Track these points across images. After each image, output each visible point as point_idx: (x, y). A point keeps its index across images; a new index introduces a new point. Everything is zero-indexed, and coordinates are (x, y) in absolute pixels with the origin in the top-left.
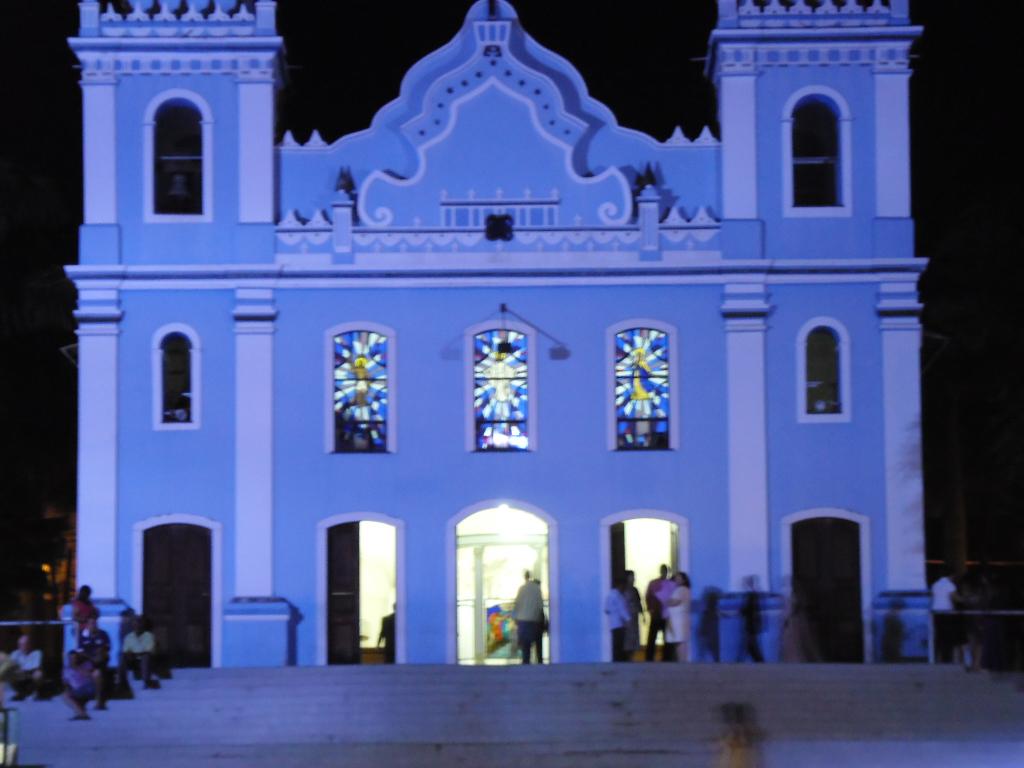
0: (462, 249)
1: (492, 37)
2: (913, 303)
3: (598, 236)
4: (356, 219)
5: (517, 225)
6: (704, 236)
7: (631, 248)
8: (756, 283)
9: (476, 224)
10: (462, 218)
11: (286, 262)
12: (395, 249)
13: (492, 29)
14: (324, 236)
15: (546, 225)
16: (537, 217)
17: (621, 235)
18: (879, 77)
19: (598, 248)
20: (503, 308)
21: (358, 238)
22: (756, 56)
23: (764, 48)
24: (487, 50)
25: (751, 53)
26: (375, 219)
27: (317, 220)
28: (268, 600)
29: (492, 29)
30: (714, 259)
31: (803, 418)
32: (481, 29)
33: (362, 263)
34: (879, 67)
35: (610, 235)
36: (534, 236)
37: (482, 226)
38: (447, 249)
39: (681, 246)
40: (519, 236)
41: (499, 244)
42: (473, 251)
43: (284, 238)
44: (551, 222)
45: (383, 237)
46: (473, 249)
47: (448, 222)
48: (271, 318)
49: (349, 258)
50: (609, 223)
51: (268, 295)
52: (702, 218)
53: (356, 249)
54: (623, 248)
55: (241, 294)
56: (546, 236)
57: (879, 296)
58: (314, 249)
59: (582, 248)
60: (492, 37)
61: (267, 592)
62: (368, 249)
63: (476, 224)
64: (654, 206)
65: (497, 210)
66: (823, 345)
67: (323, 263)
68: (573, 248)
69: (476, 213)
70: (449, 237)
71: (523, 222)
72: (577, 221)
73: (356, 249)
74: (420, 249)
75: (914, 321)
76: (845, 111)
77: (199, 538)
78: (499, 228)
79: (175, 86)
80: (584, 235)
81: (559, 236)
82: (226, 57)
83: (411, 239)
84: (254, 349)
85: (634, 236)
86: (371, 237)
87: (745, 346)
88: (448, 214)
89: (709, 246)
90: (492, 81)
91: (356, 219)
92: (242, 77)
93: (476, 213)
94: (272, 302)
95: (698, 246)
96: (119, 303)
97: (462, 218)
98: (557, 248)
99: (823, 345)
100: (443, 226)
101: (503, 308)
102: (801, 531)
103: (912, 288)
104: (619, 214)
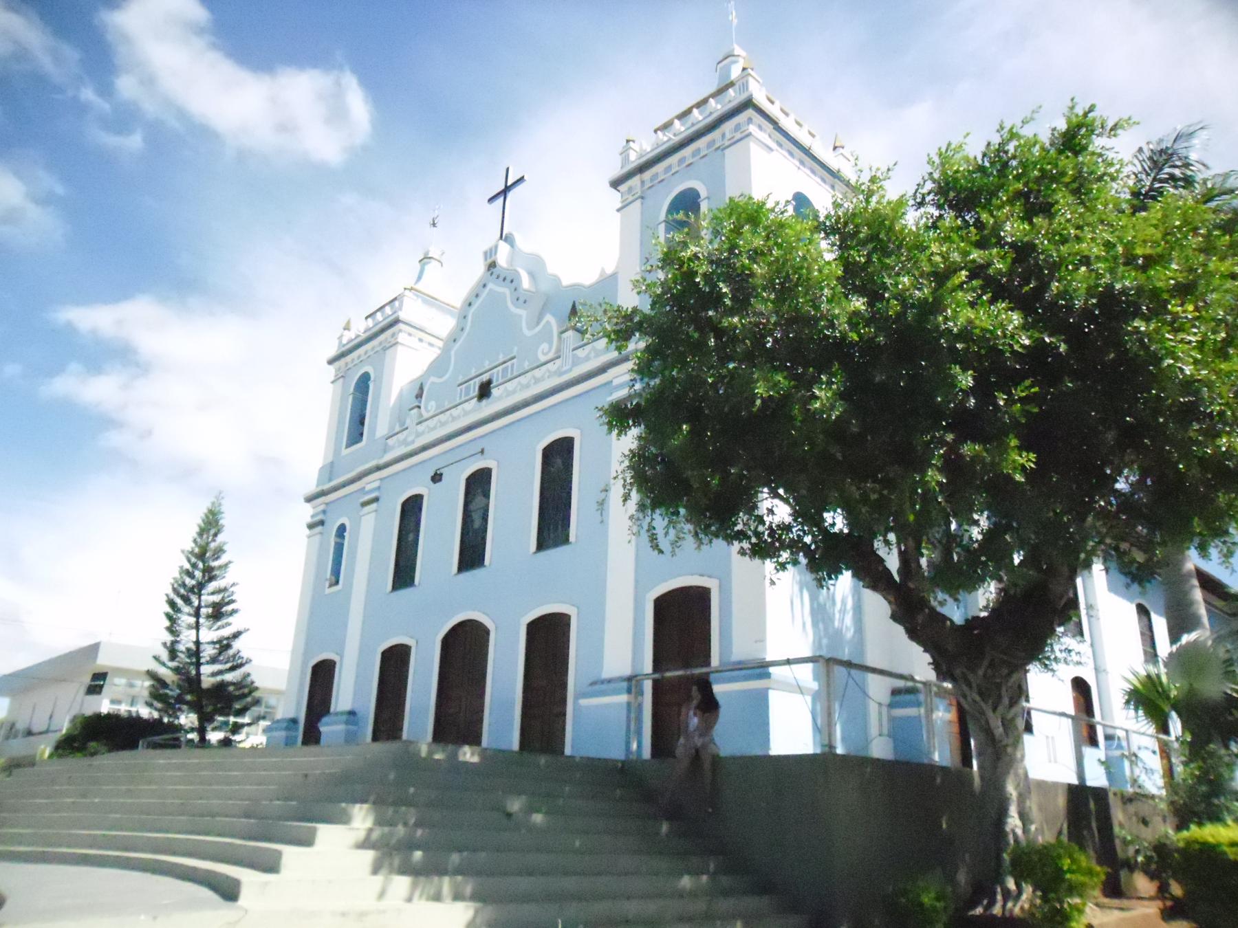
0: (466, 413)
15: (509, 376)
19: (537, 381)
20: (482, 452)
21: (421, 428)
22: (643, 182)
23: (647, 175)
25: (639, 184)
33: (419, 443)
37: (477, 392)
39: (587, 359)
40: (495, 392)
41: (484, 402)
45: (431, 423)
48: (376, 500)
50: (543, 359)
51: (376, 484)
53: (418, 435)
54: (551, 374)
59: (527, 386)
65: (485, 378)
72: (526, 366)
76: (703, 193)
78: (485, 391)
82: (382, 337)
85: (558, 362)
94: (379, 488)
96: (324, 512)
97: (467, 393)
100: (458, 401)
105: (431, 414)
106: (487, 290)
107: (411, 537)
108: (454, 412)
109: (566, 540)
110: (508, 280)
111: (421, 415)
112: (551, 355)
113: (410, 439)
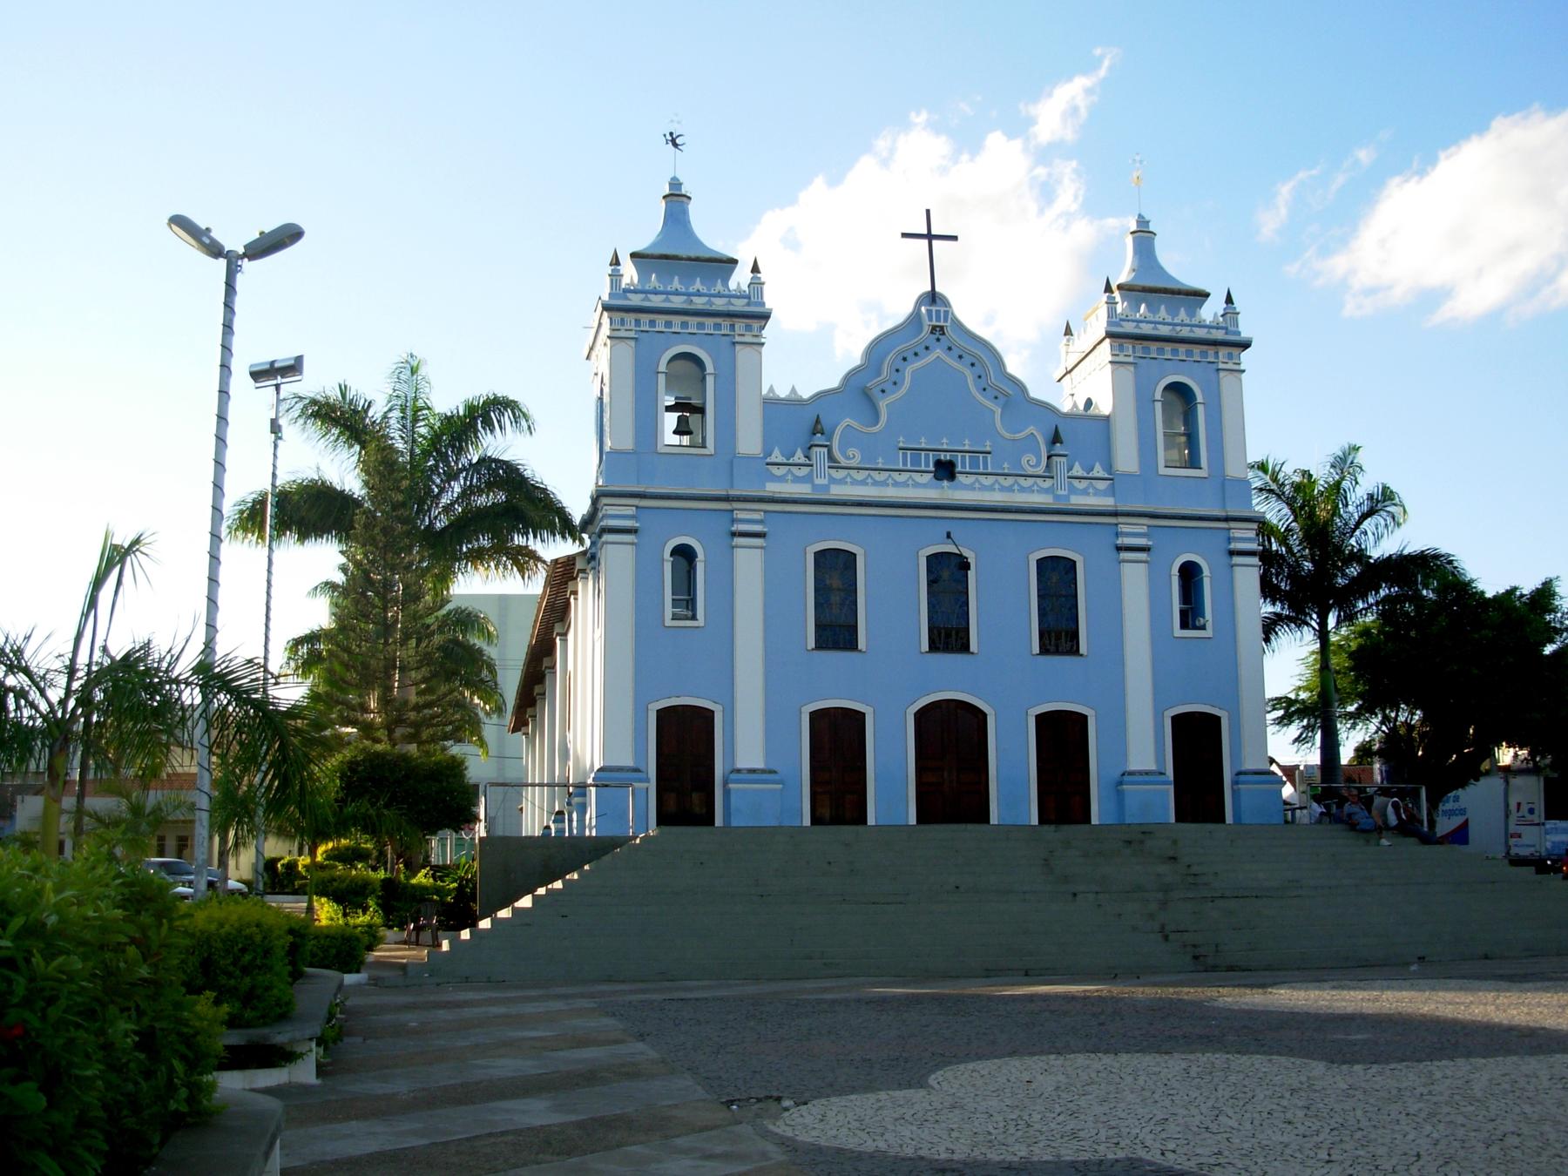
0: (917, 485)
1: (938, 319)
2: (1254, 546)
3: (1021, 480)
4: (831, 458)
5: (959, 469)
6: (1102, 485)
7: (1047, 491)
8: (1140, 526)
9: (927, 465)
10: (916, 461)
11: (773, 488)
12: (863, 483)
13: (938, 312)
14: (805, 470)
16: (974, 463)
17: (1039, 481)
18: (1222, 374)
19: (1022, 490)
20: (949, 536)
21: (833, 472)
24: (934, 328)
26: (848, 458)
27: (799, 457)
28: (763, 771)
29: (938, 312)
30: (1107, 502)
31: (1178, 632)
32: (929, 312)
33: (837, 491)
34: (1221, 366)
35: (1030, 481)
36: (972, 478)
37: (932, 468)
38: (905, 484)
39: (1085, 492)
40: (960, 478)
41: (945, 483)
42: (927, 489)
43: (774, 470)
44: (986, 466)
46: (924, 486)
47: (905, 463)
49: (826, 488)
50: (1031, 471)
52: (1098, 471)
53: (833, 480)
55: (741, 515)
56: (982, 478)
57: (1229, 540)
58: (797, 480)
59: (1010, 489)
60: (938, 319)
61: (760, 765)
62: (842, 482)
63: (927, 465)
64: (1063, 459)
66: (1189, 573)
67: (803, 490)
68: (1003, 489)
69: (927, 457)
70: (905, 476)
71: (963, 465)
72: (1006, 468)
73: (833, 480)
74: (884, 484)
75: (1255, 560)
76: (1199, 399)
77: (703, 719)
78: (946, 470)
79: (683, 343)
80: (1010, 480)
81: (991, 479)
83: (877, 476)
84: (749, 562)
85: (1049, 483)
86: (843, 473)
87: (1134, 578)
88: (905, 456)
89: (1104, 493)
90: (938, 352)
91: (831, 458)
92: (738, 339)
93: (927, 457)
95: (1097, 493)
97: (916, 461)
98: (991, 488)
99: (1189, 573)
101: (949, 536)
102: (1178, 721)
103: (1252, 534)
104: (1038, 464)
105: (853, 463)
106: (931, 357)
107: (835, 598)
108: (904, 477)
109: (1074, 650)
110: (968, 359)
111: (835, 461)
112: (1040, 470)
113: (818, 481)
